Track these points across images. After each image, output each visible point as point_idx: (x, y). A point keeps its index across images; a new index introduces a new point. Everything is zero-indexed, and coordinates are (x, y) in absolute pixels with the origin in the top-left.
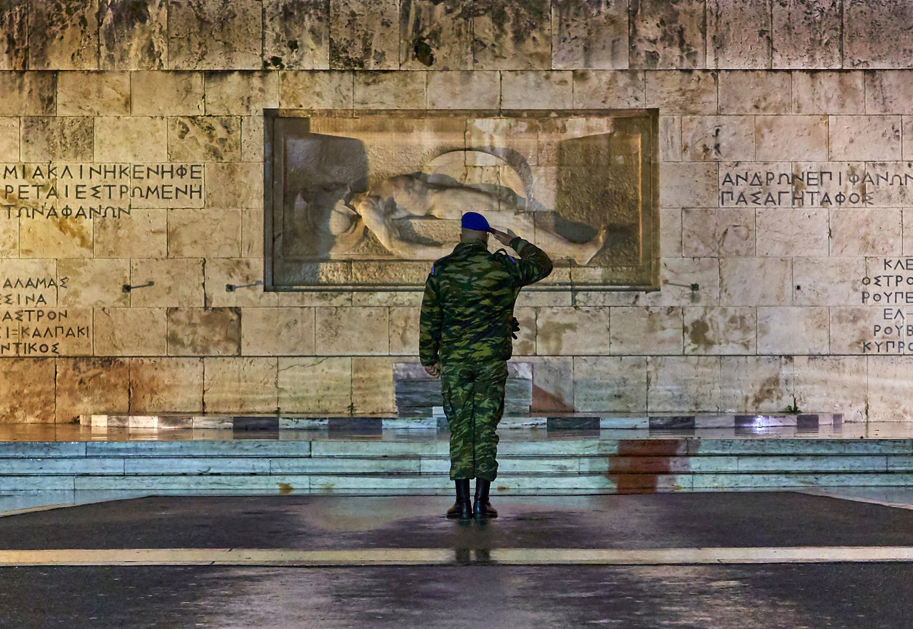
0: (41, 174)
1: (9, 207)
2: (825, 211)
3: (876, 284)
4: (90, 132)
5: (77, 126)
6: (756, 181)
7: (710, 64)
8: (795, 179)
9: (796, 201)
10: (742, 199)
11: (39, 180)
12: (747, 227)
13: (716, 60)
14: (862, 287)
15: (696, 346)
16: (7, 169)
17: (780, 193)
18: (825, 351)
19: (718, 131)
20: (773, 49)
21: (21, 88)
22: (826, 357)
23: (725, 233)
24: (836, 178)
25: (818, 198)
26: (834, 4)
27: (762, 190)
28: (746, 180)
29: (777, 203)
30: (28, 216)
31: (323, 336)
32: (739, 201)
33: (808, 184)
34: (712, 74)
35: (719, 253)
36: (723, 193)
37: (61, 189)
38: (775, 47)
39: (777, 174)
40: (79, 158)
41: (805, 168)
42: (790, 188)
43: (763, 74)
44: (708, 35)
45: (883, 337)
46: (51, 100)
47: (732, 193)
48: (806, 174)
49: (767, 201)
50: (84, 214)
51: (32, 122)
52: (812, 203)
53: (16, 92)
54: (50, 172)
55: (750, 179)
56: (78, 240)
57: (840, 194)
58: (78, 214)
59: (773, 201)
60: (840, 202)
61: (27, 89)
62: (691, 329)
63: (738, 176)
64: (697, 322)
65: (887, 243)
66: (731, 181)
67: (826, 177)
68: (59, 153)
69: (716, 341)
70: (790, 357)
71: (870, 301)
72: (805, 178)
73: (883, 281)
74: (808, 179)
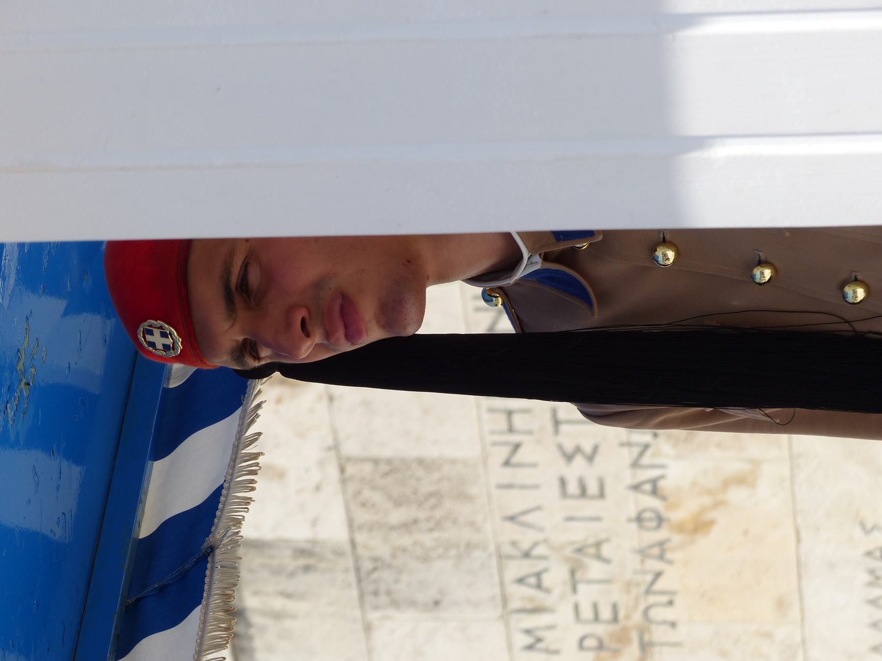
0: (538, 575)
1: (645, 646)
4: (392, 467)
5: (377, 497)
11: (556, 576)
16: (530, 647)
21: (278, 616)
30: (671, 603)
37: (579, 533)
40: (473, 490)
46: (301, 552)
50: (654, 482)
51: (376, 593)
53: (288, 623)
54: (527, 555)
56: (736, 495)
58: (655, 492)
61: (278, 603)
68: (466, 535)
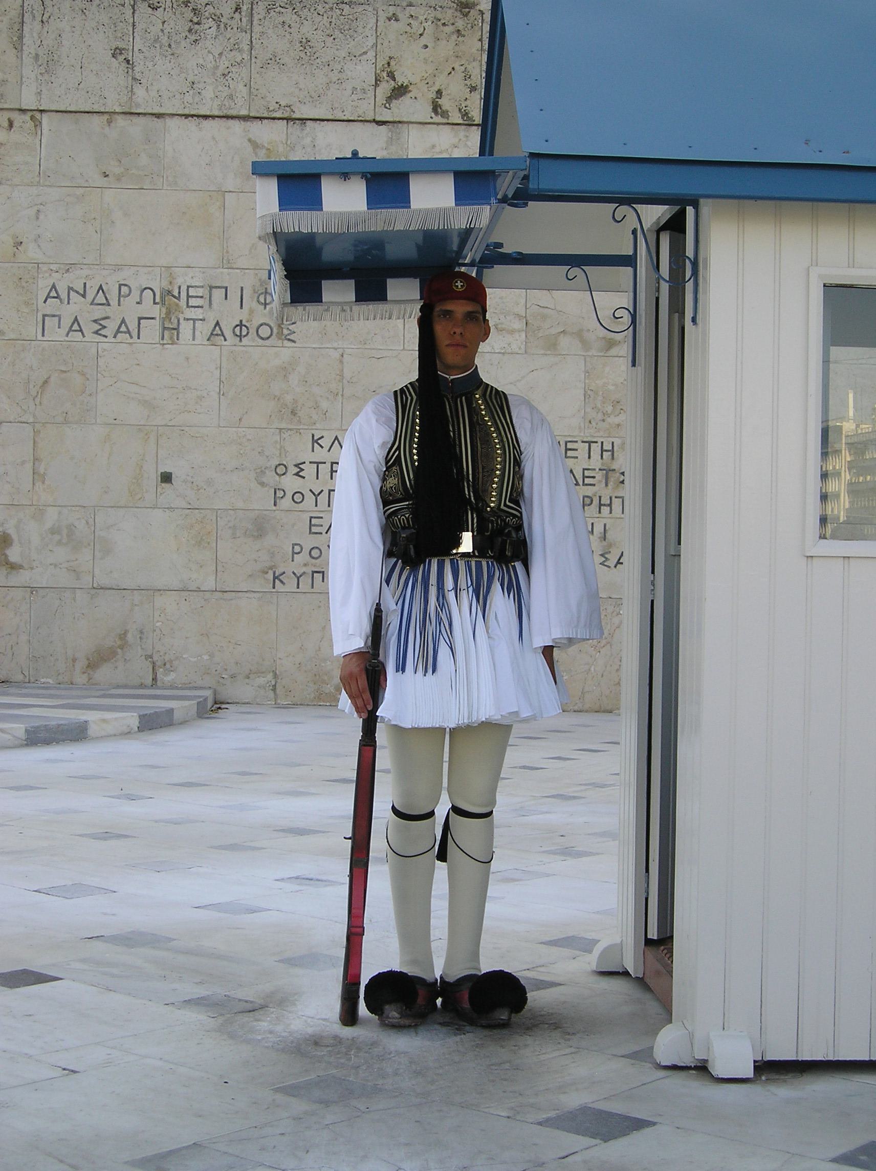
2: (216, 350)
3: (297, 474)
6: (101, 299)
7: (29, 100)
8: (167, 298)
9: (166, 333)
10: (76, 327)
12: (83, 374)
13: (39, 93)
14: (270, 478)
17: (140, 319)
18: (210, 584)
20: (134, 79)
22: (208, 595)
24: (234, 296)
25: (204, 329)
26: (238, 9)
28: (84, 296)
29: (135, 334)
32: (70, 330)
33: (188, 306)
34: (32, 118)
35: (34, 416)
36: (44, 316)
38: (138, 76)
41: (183, 279)
42: (156, 311)
43: (121, 121)
44: (25, 53)
45: (305, 565)
47: (59, 317)
48: (184, 288)
49: (118, 331)
52: (194, 339)
55: (90, 295)
57: (241, 325)
59: (129, 332)
60: (240, 337)
63: (70, 289)
65: (317, 407)
67: (218, 294)
69: (26, 566)
71: (286, 503)
72: (184, 295)
73: (309, 470)
74: (188, 296)
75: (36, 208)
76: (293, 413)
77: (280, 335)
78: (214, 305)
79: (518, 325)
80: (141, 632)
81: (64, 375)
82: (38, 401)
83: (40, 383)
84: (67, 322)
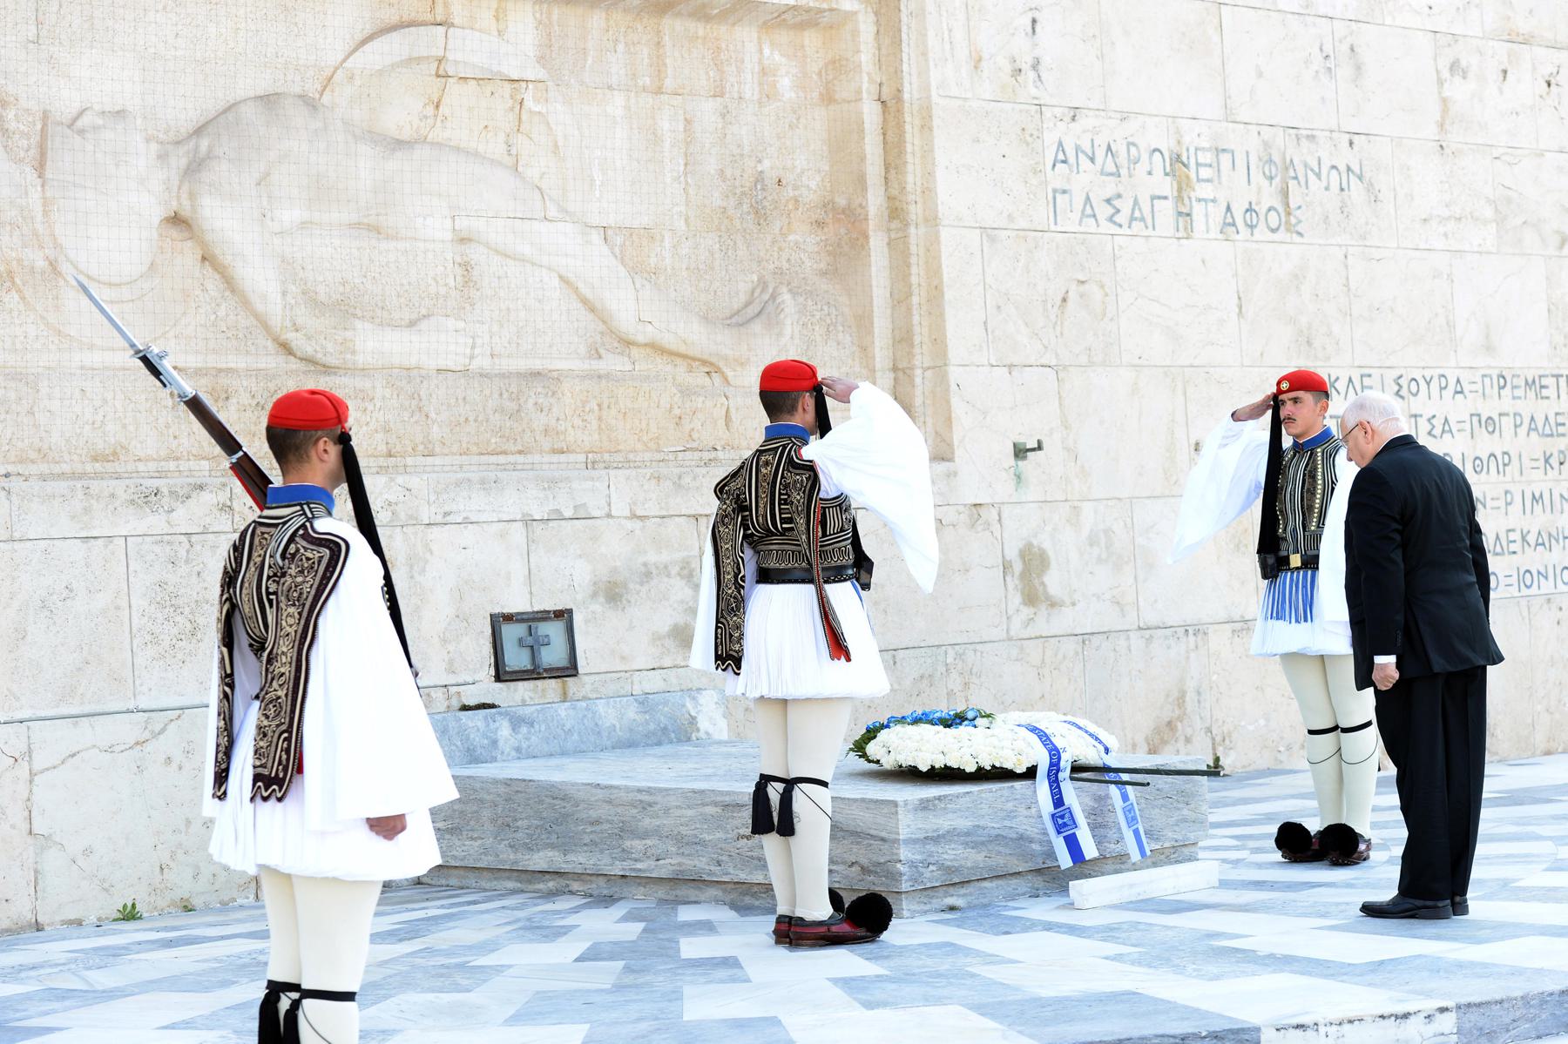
6: (1111, 168)
10: (1088, 211)
15: (1032, 610)
17: (1153, 198)
19: (1034, 21)
23: (1064, 300)
25: (1217, 213)
27: (1121, 189)
31: (155, 639)
36: (1055, 191)
39: (1142, 146)
42: (1167, 186)
48: (1192, 151)
49: (1132, 219)
59: (1143, 219)
60: (1252, 227)
62: (1018, 567)
63: (1078, 149)
64: (1029, 546)
66: (1064, 162)
67: (1225, 159)
69: (1068, 602)
70: (1195, 630)
72: (1192, 161)
74: (1198, 164)
75: (1030, 15)
76: (1309, 343)
77: (1289, 228)
78: (1224, 179)
79: (1489, 213)
80: (1199, 693)
81: (1082, 288)
82: (1058, 328)
83: (1059, 302)
84: (1079, 201)
